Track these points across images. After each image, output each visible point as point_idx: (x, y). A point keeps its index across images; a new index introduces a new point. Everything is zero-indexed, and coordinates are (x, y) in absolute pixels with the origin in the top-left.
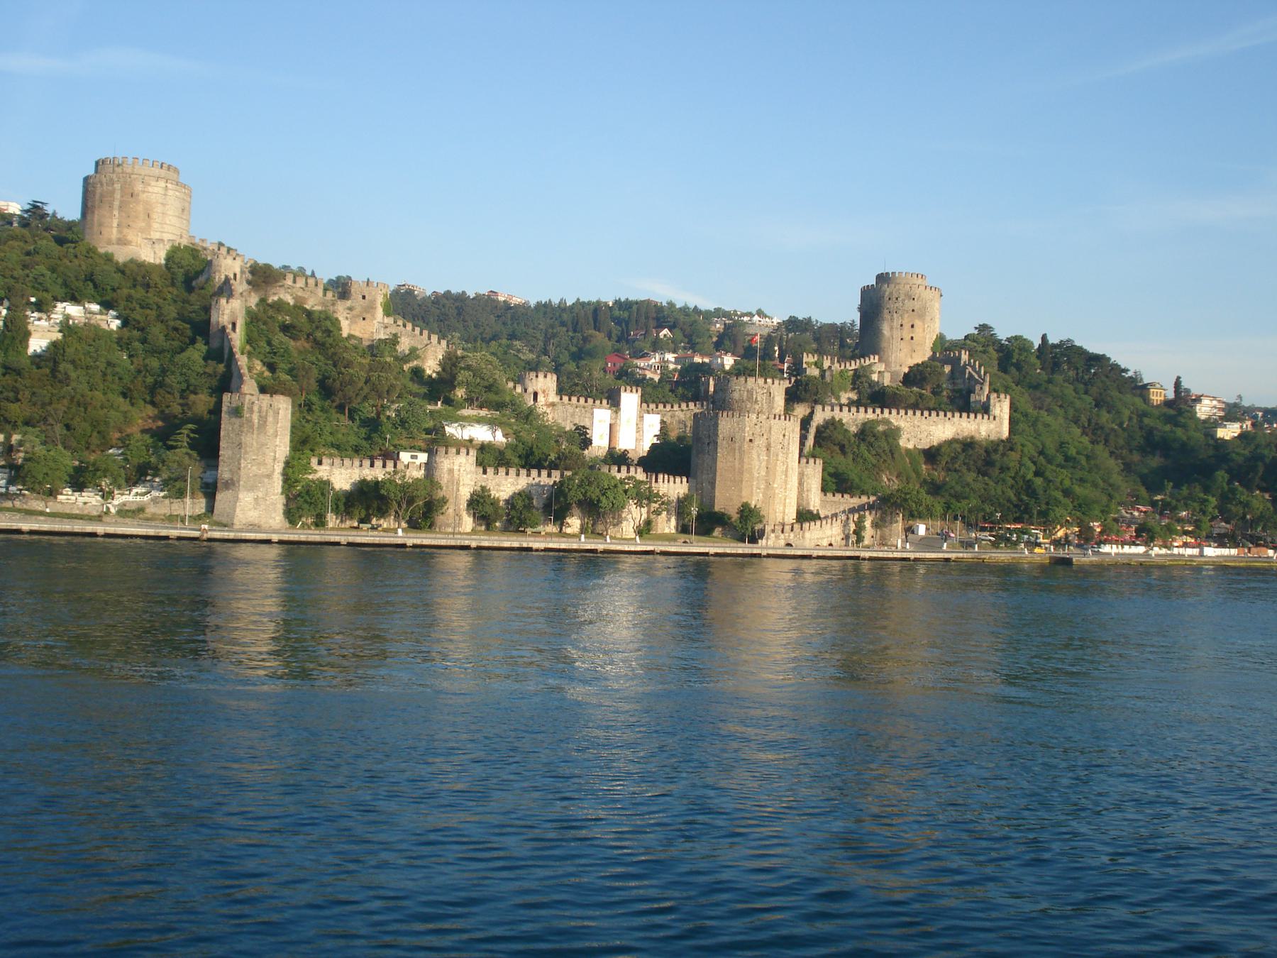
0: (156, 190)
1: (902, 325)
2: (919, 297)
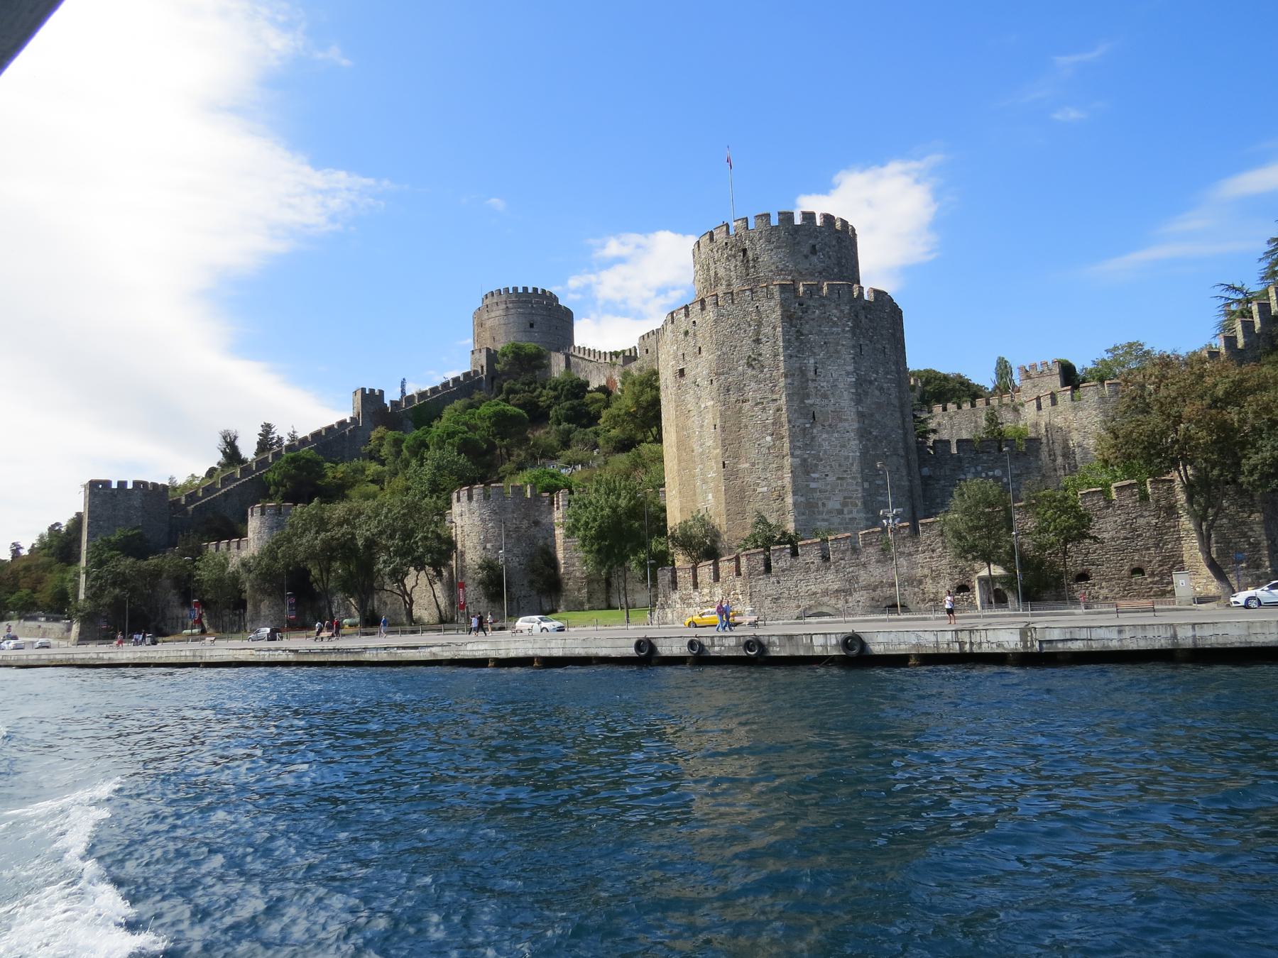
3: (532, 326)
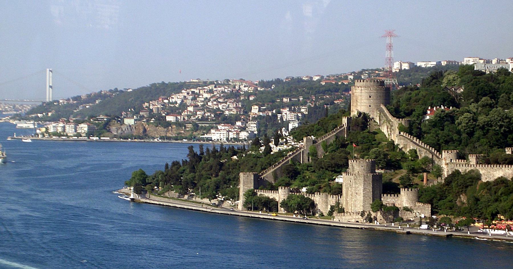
0: (358, 91)
3: (370, 97)
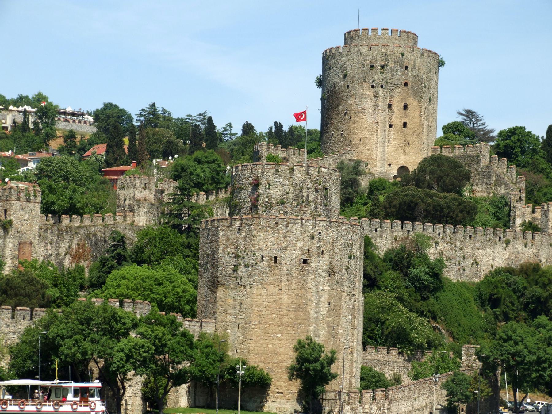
1: (390, 106)
2: (414, 65)
